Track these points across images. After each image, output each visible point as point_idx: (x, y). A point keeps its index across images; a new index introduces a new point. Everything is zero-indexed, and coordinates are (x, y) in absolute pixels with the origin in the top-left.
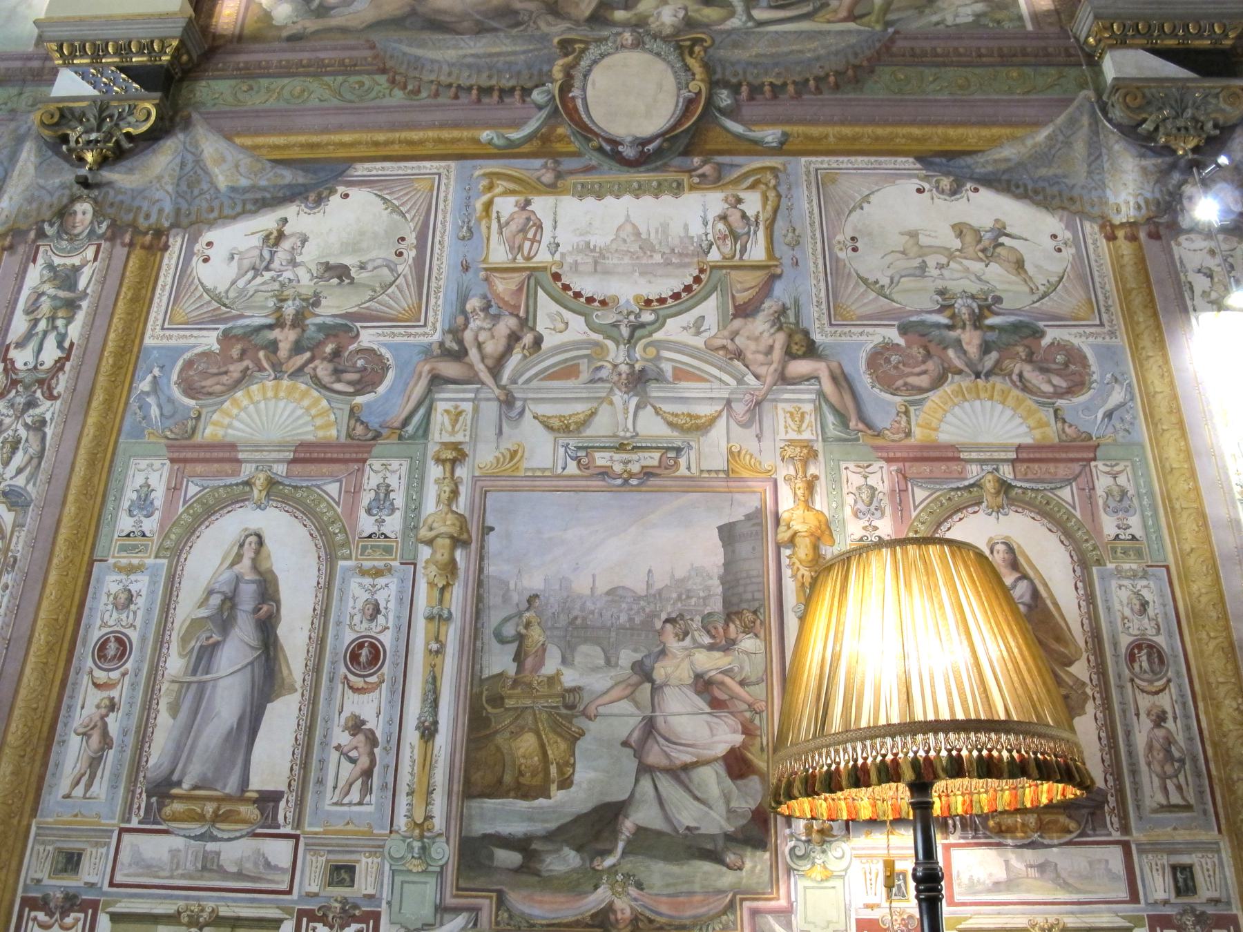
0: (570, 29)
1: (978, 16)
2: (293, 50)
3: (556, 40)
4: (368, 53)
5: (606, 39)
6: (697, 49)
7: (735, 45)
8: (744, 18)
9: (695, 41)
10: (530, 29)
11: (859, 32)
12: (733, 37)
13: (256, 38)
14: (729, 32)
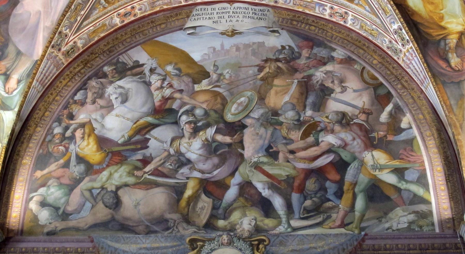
0: (195, 232)
1: (411, 223)
2: (51, 242)
3: (188, 240)
4: (90, 245)
5: (214, 239)
6: (261, 246)
7: (281, 243)
8: (286, 226)
9: (261, 241)
10: (174, 232)
11: (346, 234)
12: (280, 238)
13: (31, 233)
14: (278, 235)
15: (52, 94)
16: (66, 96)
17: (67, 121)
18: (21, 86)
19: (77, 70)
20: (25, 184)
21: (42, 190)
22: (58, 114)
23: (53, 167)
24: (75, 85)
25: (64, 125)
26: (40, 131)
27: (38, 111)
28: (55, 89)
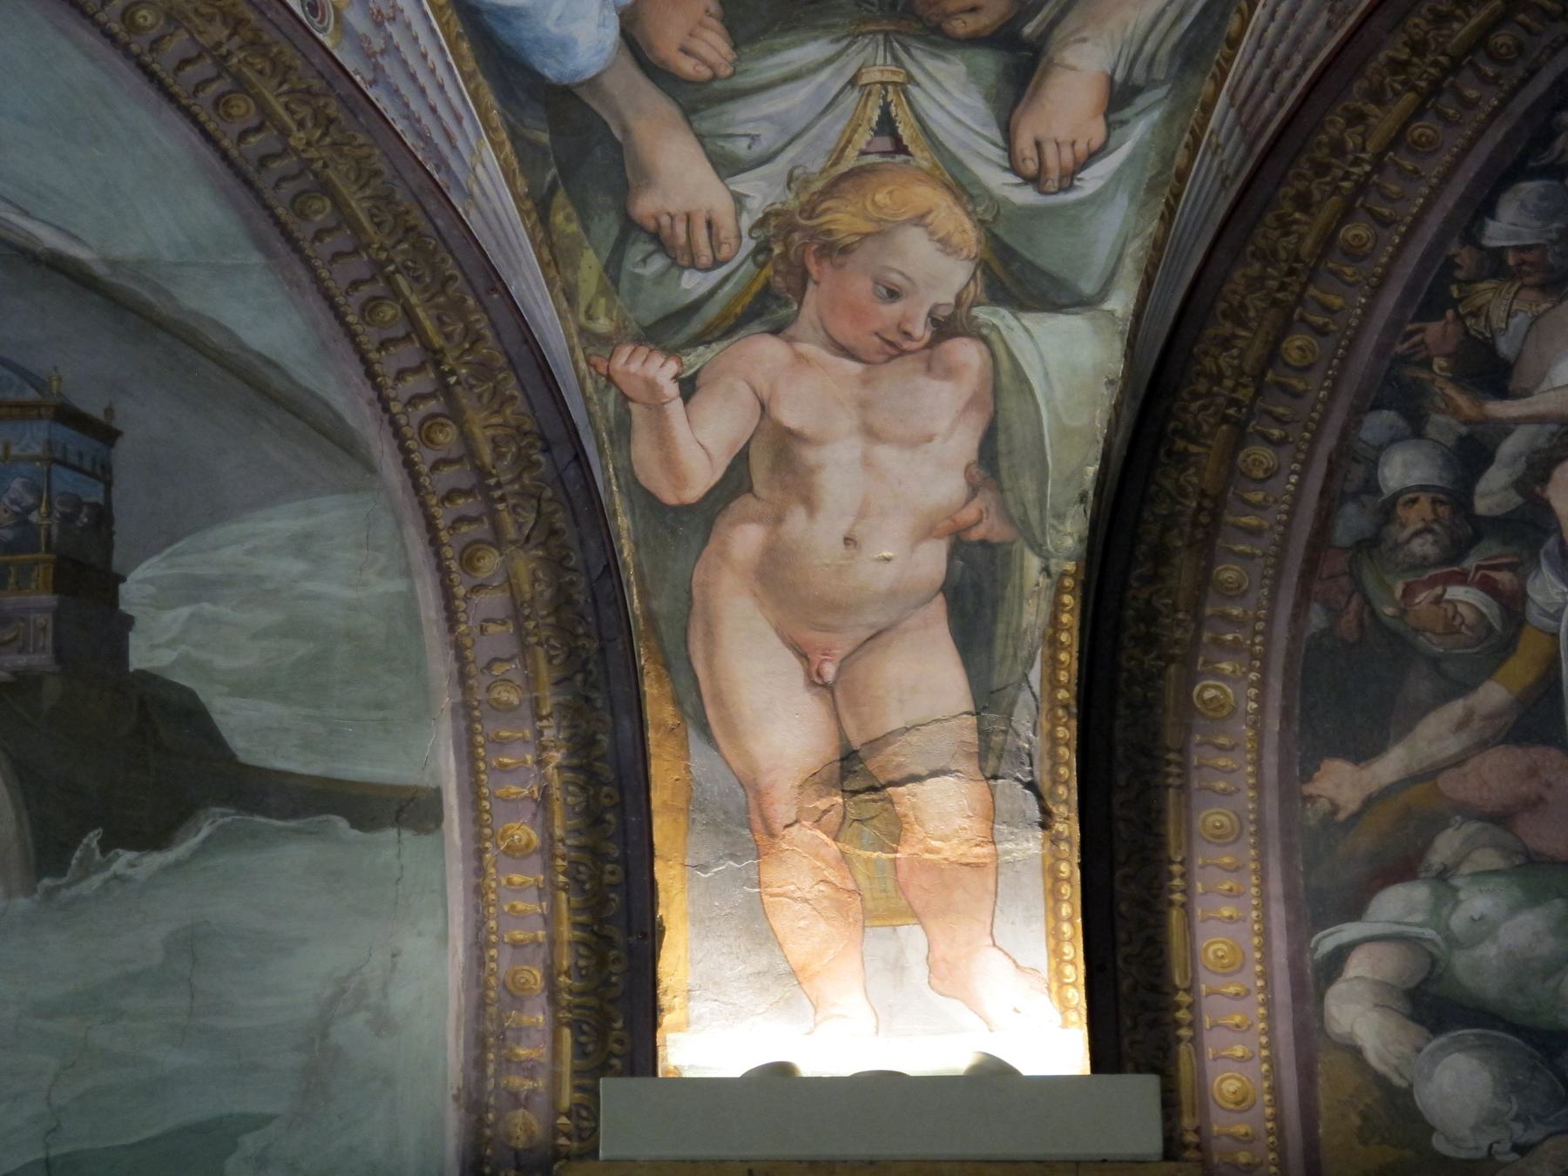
15: (1304, 202)
16: (1418, 220)
17: (1462, 401)
18: (1140, 129)
19: (1462, 30)
20: (1261, 858)
21: (1398, 905)
22: (1381, 351)
23: (1436, 735)
24: (1472, 142)
25: (1442, 426)
26: (1271, 474)
27: (1227, 327)
28: (1322, 169)
